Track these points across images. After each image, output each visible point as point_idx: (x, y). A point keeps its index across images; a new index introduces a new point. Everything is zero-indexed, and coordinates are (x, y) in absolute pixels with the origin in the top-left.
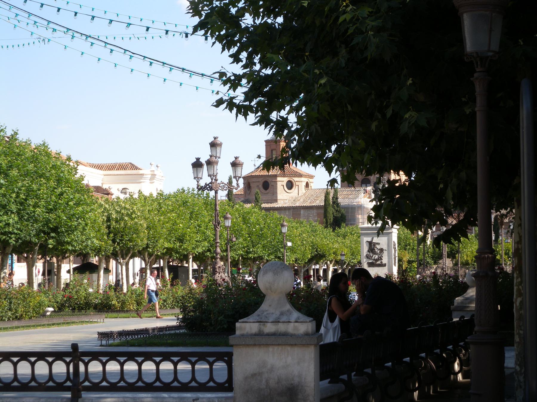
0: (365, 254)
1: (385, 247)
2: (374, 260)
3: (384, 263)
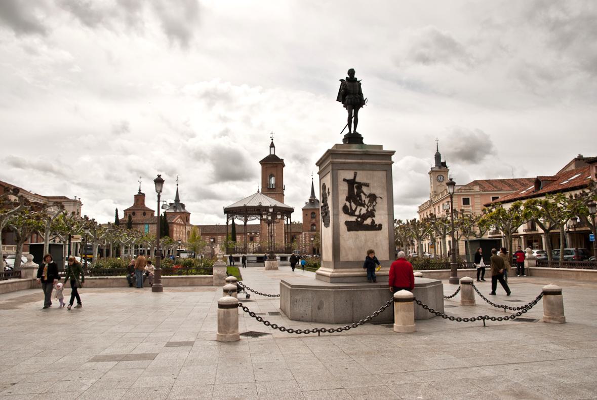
0: (341, 206)
1: (378, 192)
2: (359, 216)
3: (377, 223)
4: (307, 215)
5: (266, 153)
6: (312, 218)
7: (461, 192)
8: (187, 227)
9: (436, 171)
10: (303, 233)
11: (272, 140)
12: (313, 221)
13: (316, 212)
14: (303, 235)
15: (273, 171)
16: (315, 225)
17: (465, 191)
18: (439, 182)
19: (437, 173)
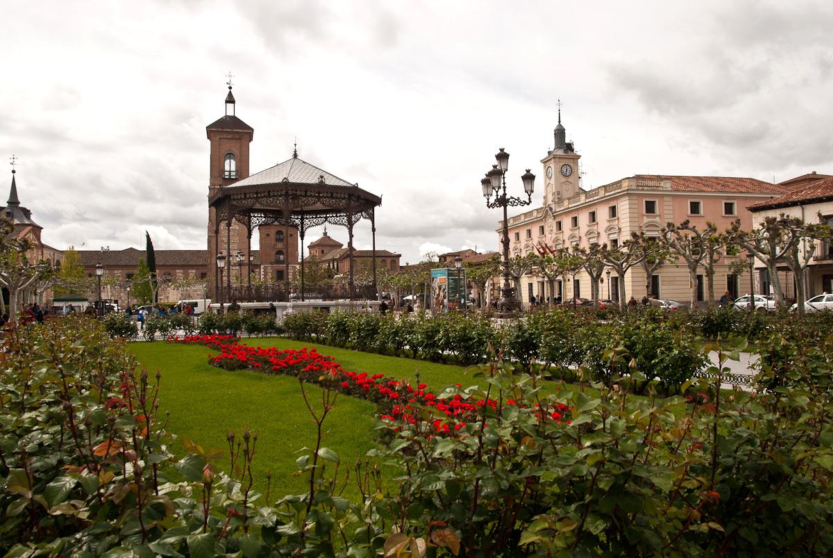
4: (268, 235)
5: (218, 111)
7: (643, 189)
8: (45, 252)
9: (560, 158)
10: (262, 267)
11: (230, 88)
12: (280, 246)
14: (262, 270)
15: (234, 147)
16: (282, 254)
17: (649, 188)
18: (565, 176)
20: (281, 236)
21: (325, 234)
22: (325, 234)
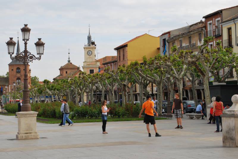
4: (12, 70)
6: (17, 72)
7: (89, 66)
12: (18, 75)
13: (20, 67)
14: (10, 88)
19: (87, 49)
20: (19, 70)
21: (69, 61)
22: (69, 61)
